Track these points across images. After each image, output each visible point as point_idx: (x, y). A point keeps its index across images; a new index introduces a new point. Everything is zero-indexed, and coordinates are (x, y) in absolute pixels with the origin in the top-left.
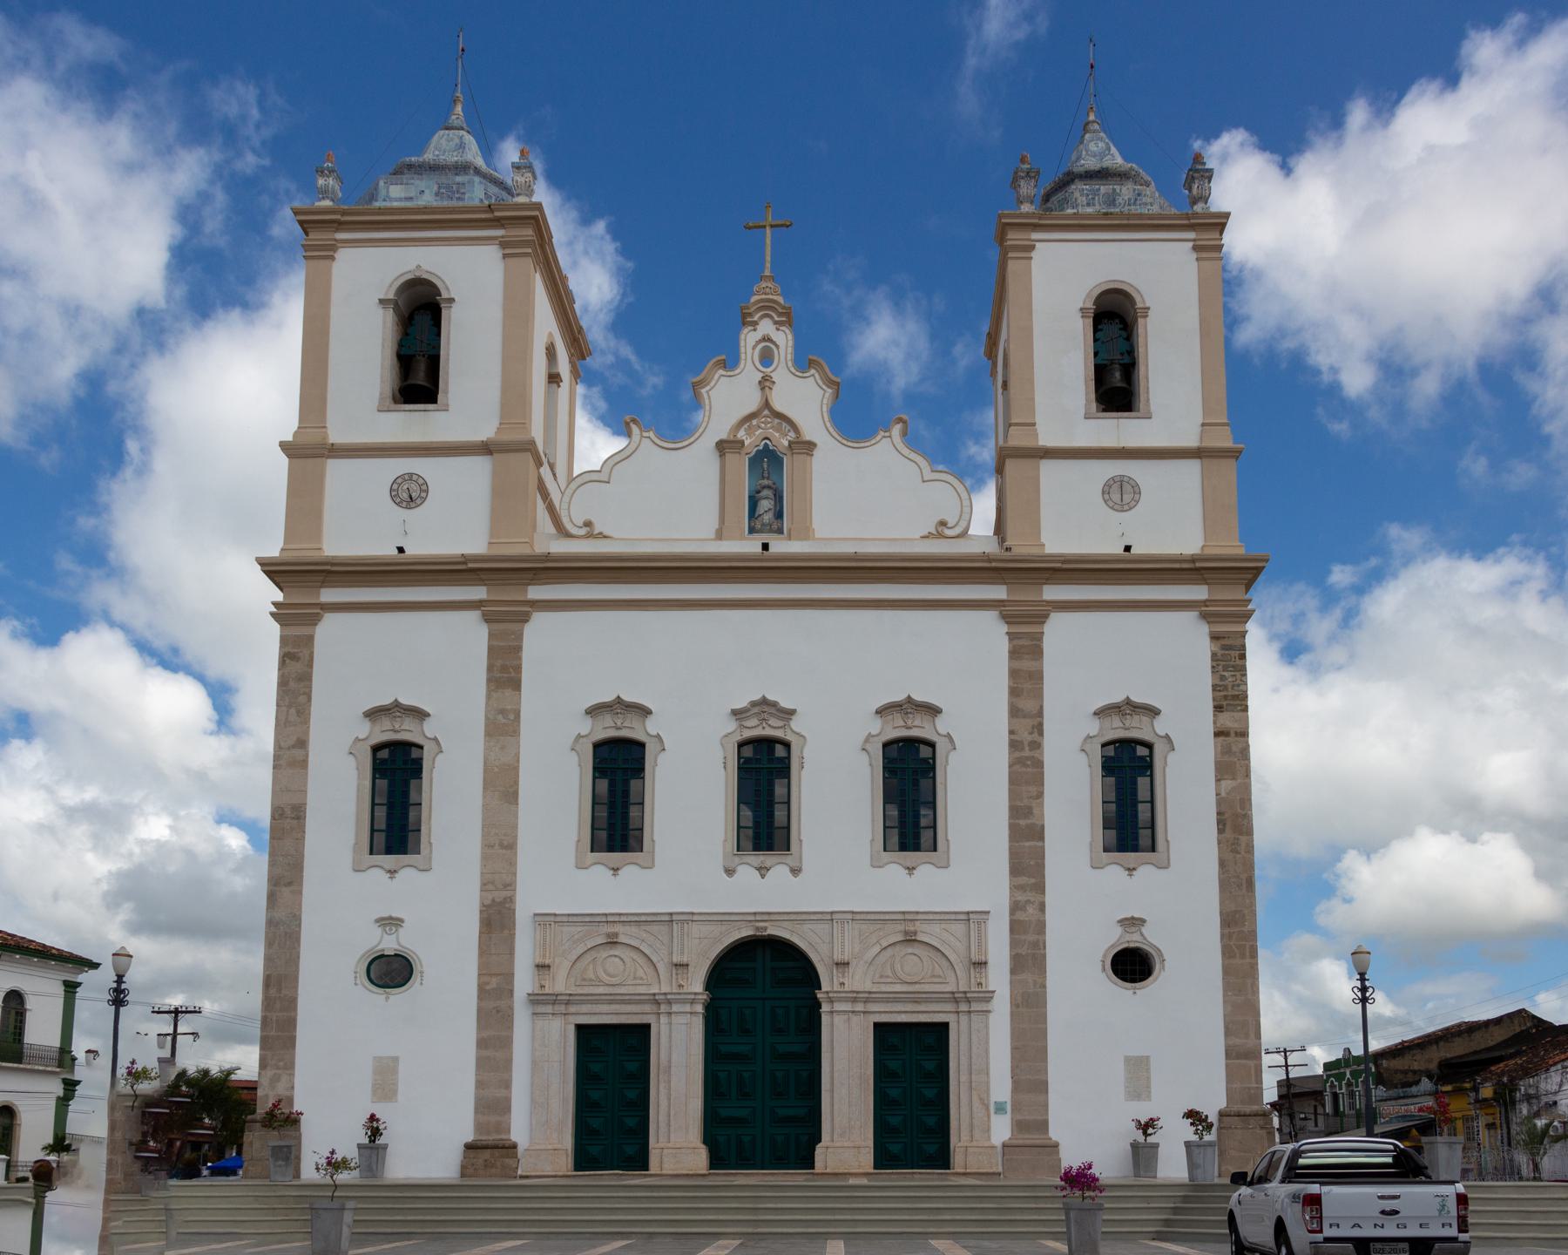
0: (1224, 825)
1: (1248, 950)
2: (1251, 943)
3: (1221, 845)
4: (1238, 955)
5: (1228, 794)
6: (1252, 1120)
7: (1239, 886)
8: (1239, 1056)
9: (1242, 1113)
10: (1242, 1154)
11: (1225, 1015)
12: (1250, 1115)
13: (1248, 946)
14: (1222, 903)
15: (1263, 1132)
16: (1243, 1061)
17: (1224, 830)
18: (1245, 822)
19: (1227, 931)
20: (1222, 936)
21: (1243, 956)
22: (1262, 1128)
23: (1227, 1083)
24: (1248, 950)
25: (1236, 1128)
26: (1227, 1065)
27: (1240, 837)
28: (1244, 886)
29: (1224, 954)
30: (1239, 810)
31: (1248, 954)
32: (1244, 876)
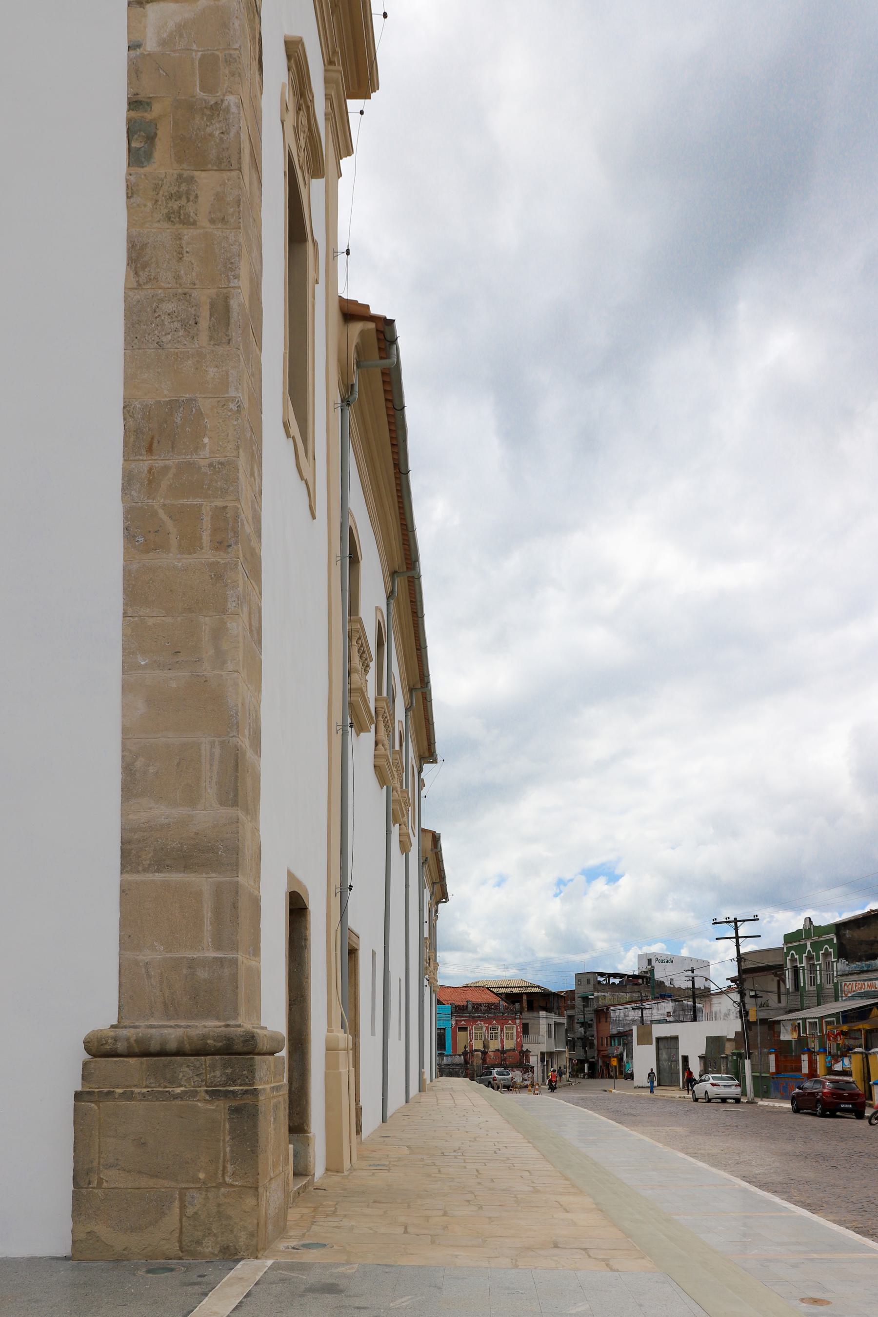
0: (151, 139)
1: (207, 522)
2: (219, 503)
3: (136, 200)
4: (174, 541)
5: (163, 43)
6: (185, 1068)
7: (190, 325)
8: (159, 865)
9: (154, 1046)
10: (145, 1182)
11: (125, 731)
12: (179, 1053)
13: (207, 511)
14: (129, 380)
15: (219, 1109)
16: (175, 877)
17: (149, 155)
18: (215, 128)
19: (143, 465)
20: (129, 480)
21: (190, 544)
22: (214, 1094)
23: (124, 945)
24: (207, 522)
25: (128, 1096)
26: (124, 891)
27: (197, 173)
28: (204, 324)
29: (129, 535)
30: (199, 93)
31: (206, 537)
32: (203, 296)
